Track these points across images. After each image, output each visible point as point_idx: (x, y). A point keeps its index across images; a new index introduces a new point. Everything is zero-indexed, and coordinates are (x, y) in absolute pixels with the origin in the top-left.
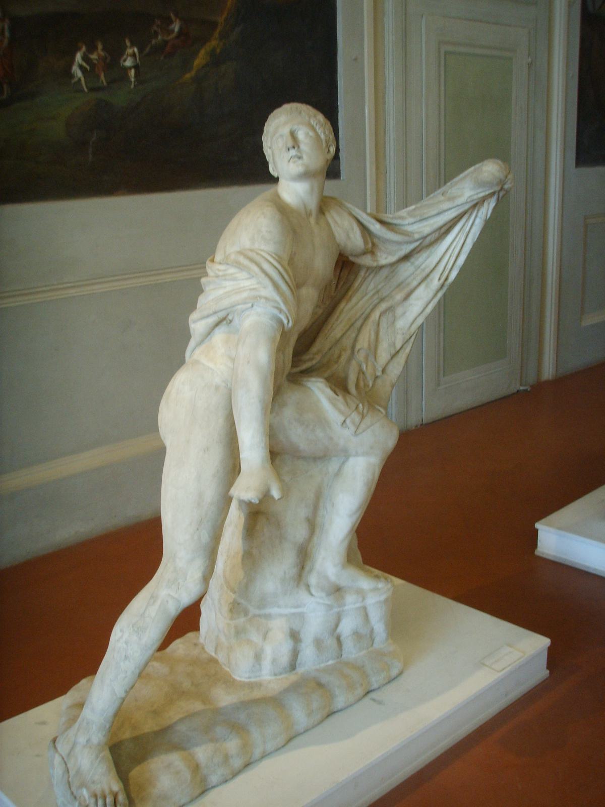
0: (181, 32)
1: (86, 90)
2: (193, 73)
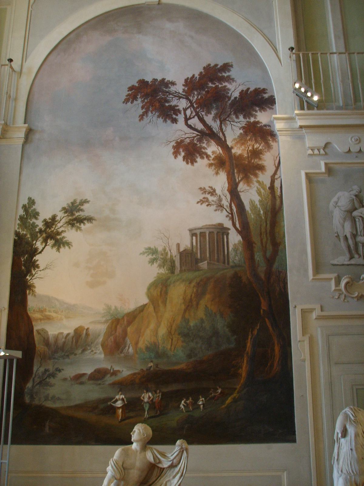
0: (221, 392)
1: (184, 412)
2: (226, 405)
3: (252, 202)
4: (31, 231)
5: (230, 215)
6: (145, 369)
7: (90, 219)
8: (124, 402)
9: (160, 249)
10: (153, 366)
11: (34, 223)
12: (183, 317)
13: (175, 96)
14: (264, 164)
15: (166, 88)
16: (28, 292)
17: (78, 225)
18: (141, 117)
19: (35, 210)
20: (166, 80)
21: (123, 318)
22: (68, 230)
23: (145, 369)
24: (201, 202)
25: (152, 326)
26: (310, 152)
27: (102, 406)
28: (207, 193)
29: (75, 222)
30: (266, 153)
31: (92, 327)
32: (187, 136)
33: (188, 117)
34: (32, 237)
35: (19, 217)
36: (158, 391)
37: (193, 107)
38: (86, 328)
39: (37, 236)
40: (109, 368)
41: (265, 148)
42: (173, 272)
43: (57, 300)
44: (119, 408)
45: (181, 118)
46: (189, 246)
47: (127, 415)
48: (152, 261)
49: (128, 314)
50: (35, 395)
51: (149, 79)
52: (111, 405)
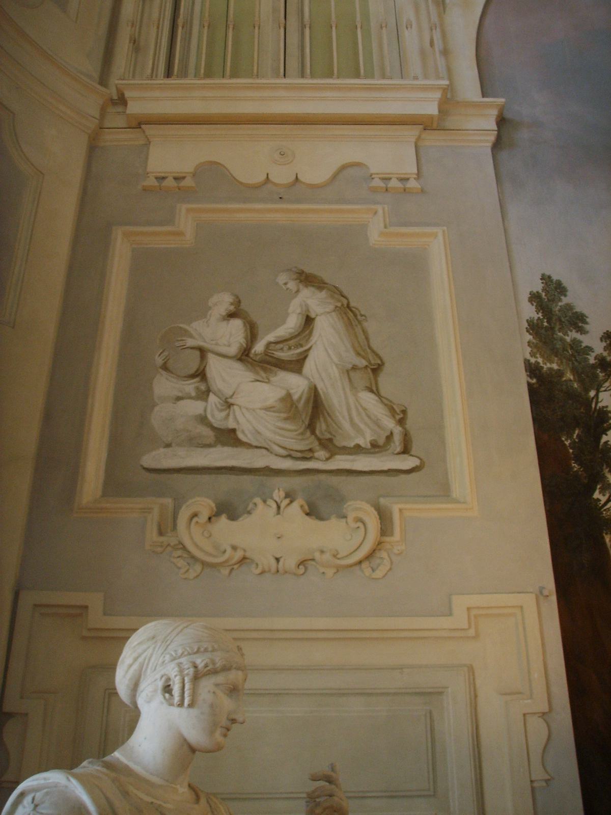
4: (573, 363)
11: (576, 343)
19: (569, 307)
34: (581, 381)
35: (526, 325)
39: (597, 376)
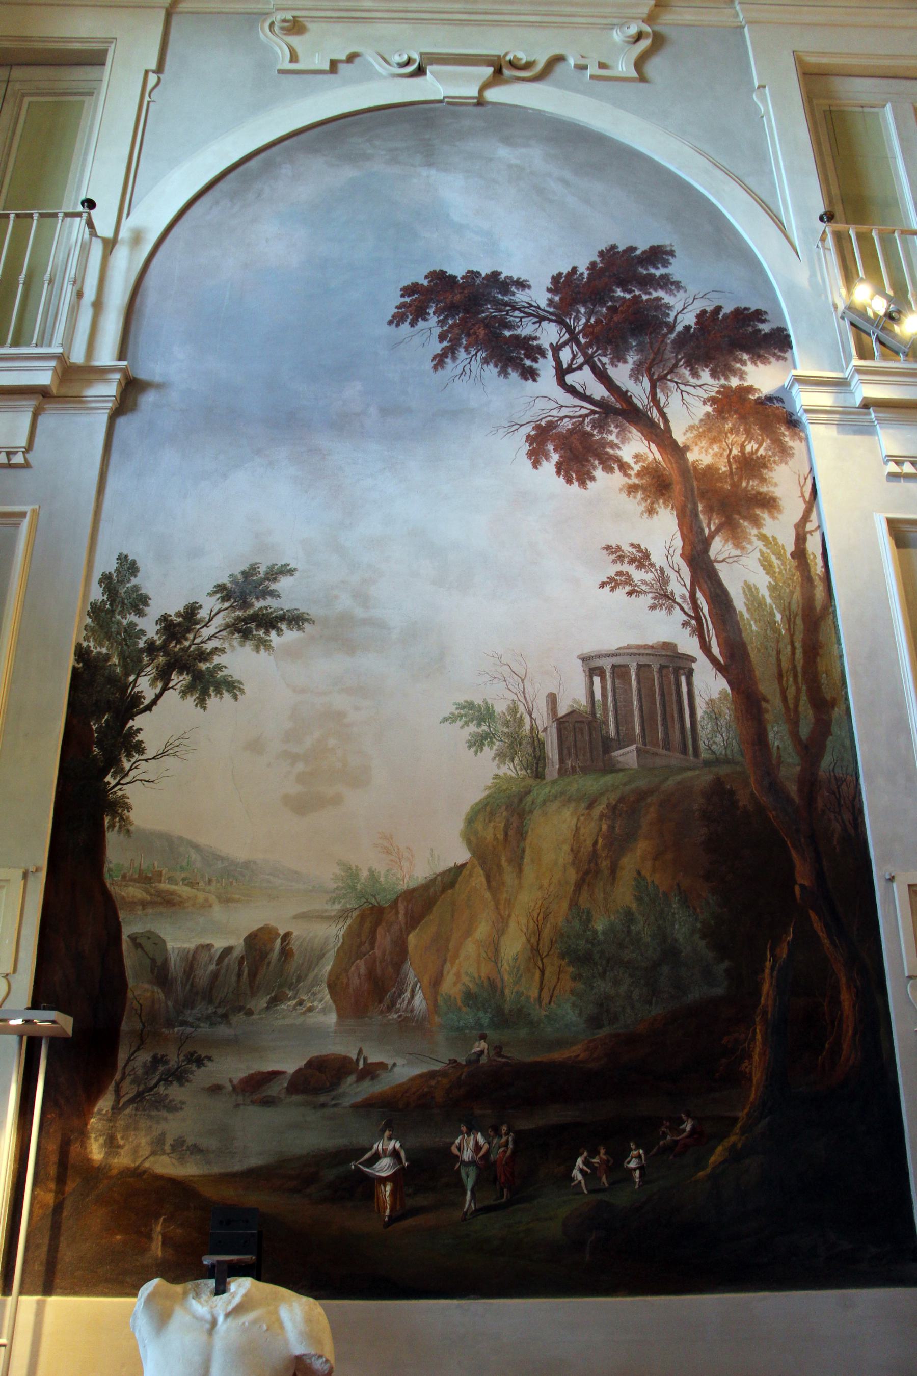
1: (586, 1192)
2: (709, 1170)
3: (750, 590)
4: (122, 647)
5: (693, 622)
6: (462, 1060)
7: (296, 620)
8: (402, 1163)
9: (500, 708)
10: (486, 1051)
11: (132, 625)
12: (573, 904)
13: (530, 315)
14: (774, 492)
15: (505, 294)
16: (107, 820)
17: (261, 633)
18: (439, 361)
19: (136, 588)
20: (503, 276)
21: (395, 904)
22: (231, 646)
23: (462, 1060)
24: (613, 583)
25: (482, 930)
26: (892, 467)
27: (330, 1175)
28: (626, 560)
29: (253, 625)
30: (777, 465)
31: (298, 931)
32: (564, 412)
33: (565, 366)
34: (125, 666)
35: (89, 608)
36: (504, 1129)
37: (578, 344)
38: (282, 932)
39: (140, 660)
40: (354, 1057)
41: (774, 454)
42: (539, 775)
43: (196, 847)
44: (384, 1180)
45: (546, 368)
46: (583, 701)
47: (410, 1202)
48: (478, 742)
49: (409, 895)
50: (122, 1138)
51: (458, 270)
52: (358, 1170)
